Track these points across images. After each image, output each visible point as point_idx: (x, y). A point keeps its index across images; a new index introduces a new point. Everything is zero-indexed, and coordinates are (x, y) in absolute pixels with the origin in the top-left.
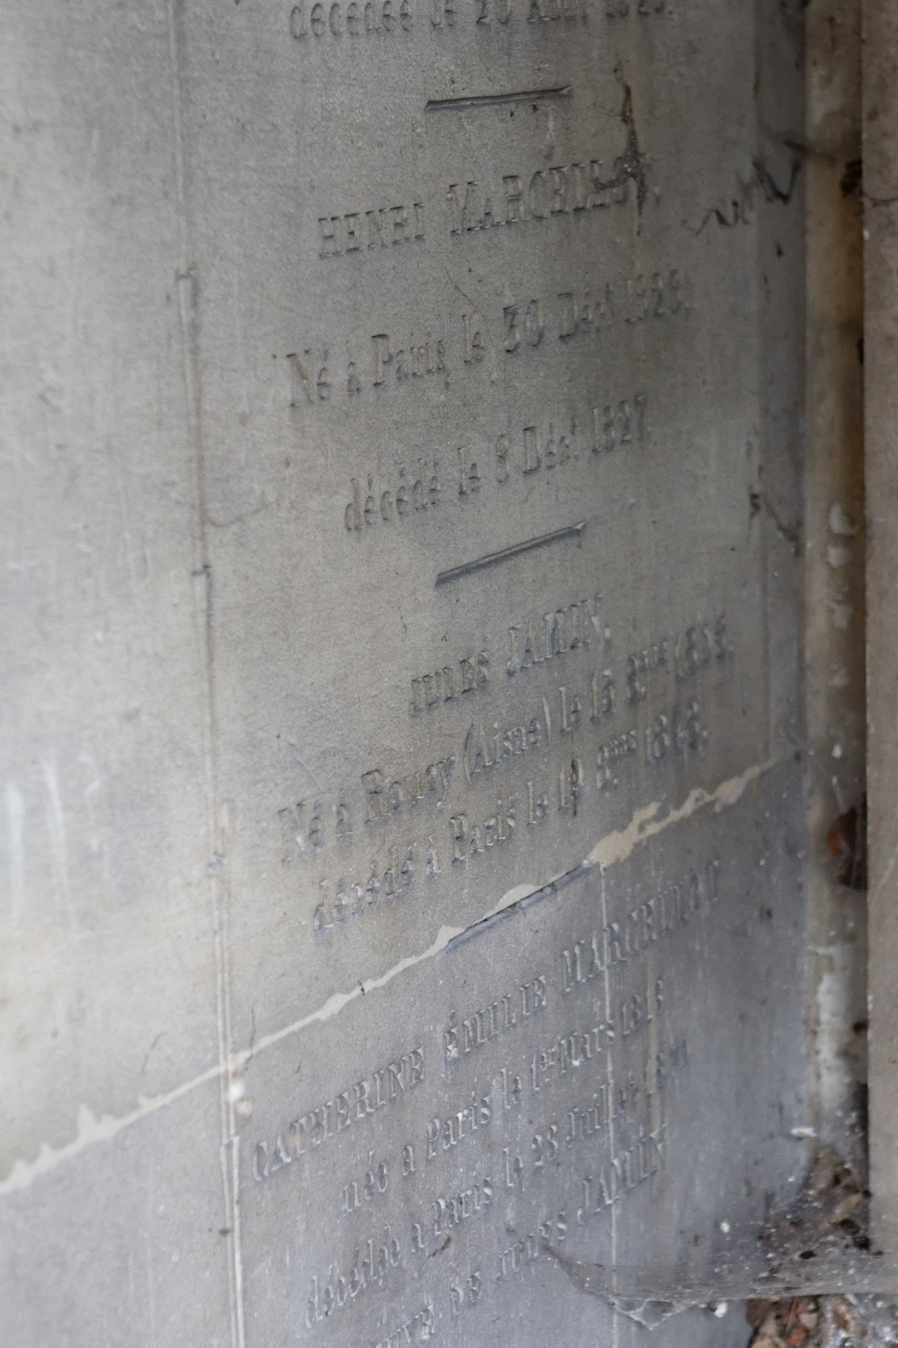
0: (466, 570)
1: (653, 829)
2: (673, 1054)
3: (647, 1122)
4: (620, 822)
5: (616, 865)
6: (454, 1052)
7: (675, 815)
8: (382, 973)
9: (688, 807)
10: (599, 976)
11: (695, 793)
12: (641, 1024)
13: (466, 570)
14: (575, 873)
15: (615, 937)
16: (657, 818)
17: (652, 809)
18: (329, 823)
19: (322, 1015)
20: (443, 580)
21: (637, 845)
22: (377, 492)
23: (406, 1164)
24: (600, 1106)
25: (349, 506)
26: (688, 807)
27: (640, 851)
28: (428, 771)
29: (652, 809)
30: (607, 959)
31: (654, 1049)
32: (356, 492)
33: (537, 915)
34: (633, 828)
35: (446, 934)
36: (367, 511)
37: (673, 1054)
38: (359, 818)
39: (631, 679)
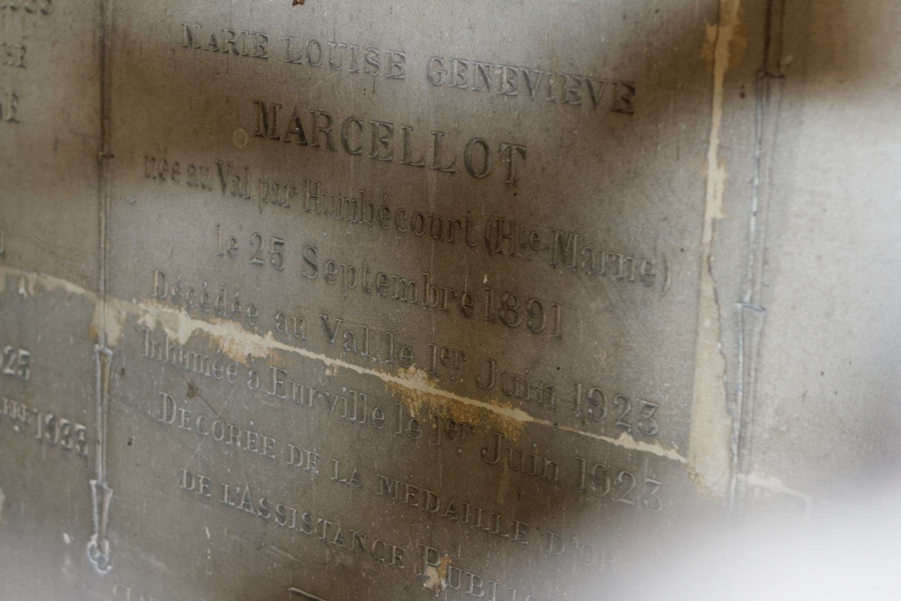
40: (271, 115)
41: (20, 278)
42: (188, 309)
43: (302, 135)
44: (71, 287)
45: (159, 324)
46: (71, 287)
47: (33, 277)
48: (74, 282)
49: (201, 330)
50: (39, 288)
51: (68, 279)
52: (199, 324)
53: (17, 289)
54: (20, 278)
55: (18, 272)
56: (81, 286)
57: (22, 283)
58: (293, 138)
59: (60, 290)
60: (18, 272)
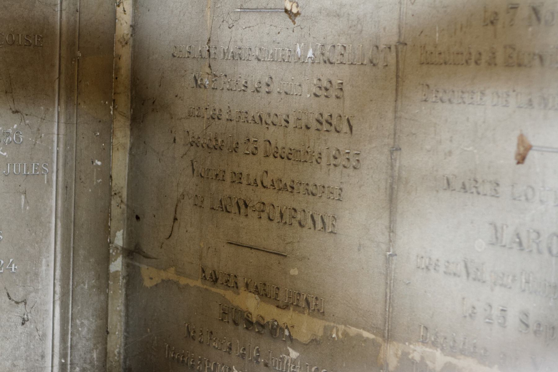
40: (500, 230)
41: (334, 327)
42: (442, 349)
43: (520, 244)
45: (422, 358)
47: (342, 327)
48: (368, 331)
49: (450, 363)
50: (345, 334)
51: (364, 329)
52: (449, 359)
53: (331, 335)
55: (332, 324)
56: (373, 333)
57: (335, 330)
58: (515, 246)
59: (359, 336)
60: (332, 324)
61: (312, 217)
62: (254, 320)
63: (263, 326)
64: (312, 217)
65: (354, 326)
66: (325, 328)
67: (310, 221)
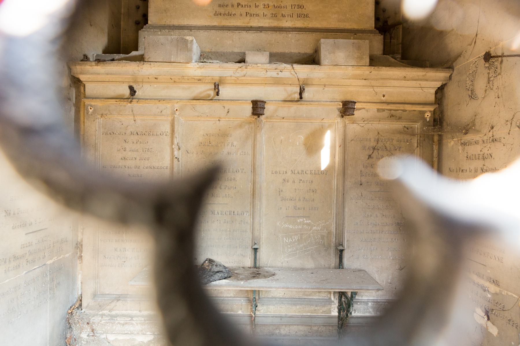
0: (30, 233)
1: (56, 260)
2: (58, 284)
3: (54, 291)
4: (51, 259)
5: (51, 264)
6: (25, 285)
7: (59, 258)
8: (15, 277)
9: (61, 257)
10: (47, 276)
11: (62, 256)
12: (53, 281)
13: (30, 233)
14: (44, 265)
15: (50, 272)
16: (57, 258)
17: (56, 257)
18: (7, 261)
19: (5, 282)
20: (26, 234)
21: (54, 261)
22: (17, 225)
23: (17, 298)
24: (47, 290)
25: (13, 227)
26: (61, 257)
27: (54, 263)
28: (23, 254)
29: (56, 257)
30: (49, 274)
31: (55, 283)
32: (14, 225)
33: (38, 270)
34: (53, 259)
35: (24, 272)
36: (16, 227)
37: (58, 284)
38: (12, 260)
39: (53, 244)
44: (514, 295)
46: (514, 295)
47: (506, 292)
48: (515, 295)
50: (507, 294)
51: (514, 294)
53: (502, 293)
54: (502, 291)
55: (502, 290)
56: (517, 296)
57: (503, 292)
60: (502, 290)
61: (495, 256)
62: (476, 283)
63: (479, 285)
64: (495, 256)
65: (510, 292)
66: (500, 290)
67: (494, 257)
